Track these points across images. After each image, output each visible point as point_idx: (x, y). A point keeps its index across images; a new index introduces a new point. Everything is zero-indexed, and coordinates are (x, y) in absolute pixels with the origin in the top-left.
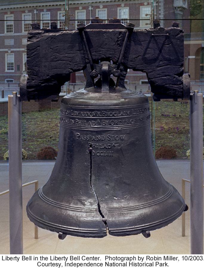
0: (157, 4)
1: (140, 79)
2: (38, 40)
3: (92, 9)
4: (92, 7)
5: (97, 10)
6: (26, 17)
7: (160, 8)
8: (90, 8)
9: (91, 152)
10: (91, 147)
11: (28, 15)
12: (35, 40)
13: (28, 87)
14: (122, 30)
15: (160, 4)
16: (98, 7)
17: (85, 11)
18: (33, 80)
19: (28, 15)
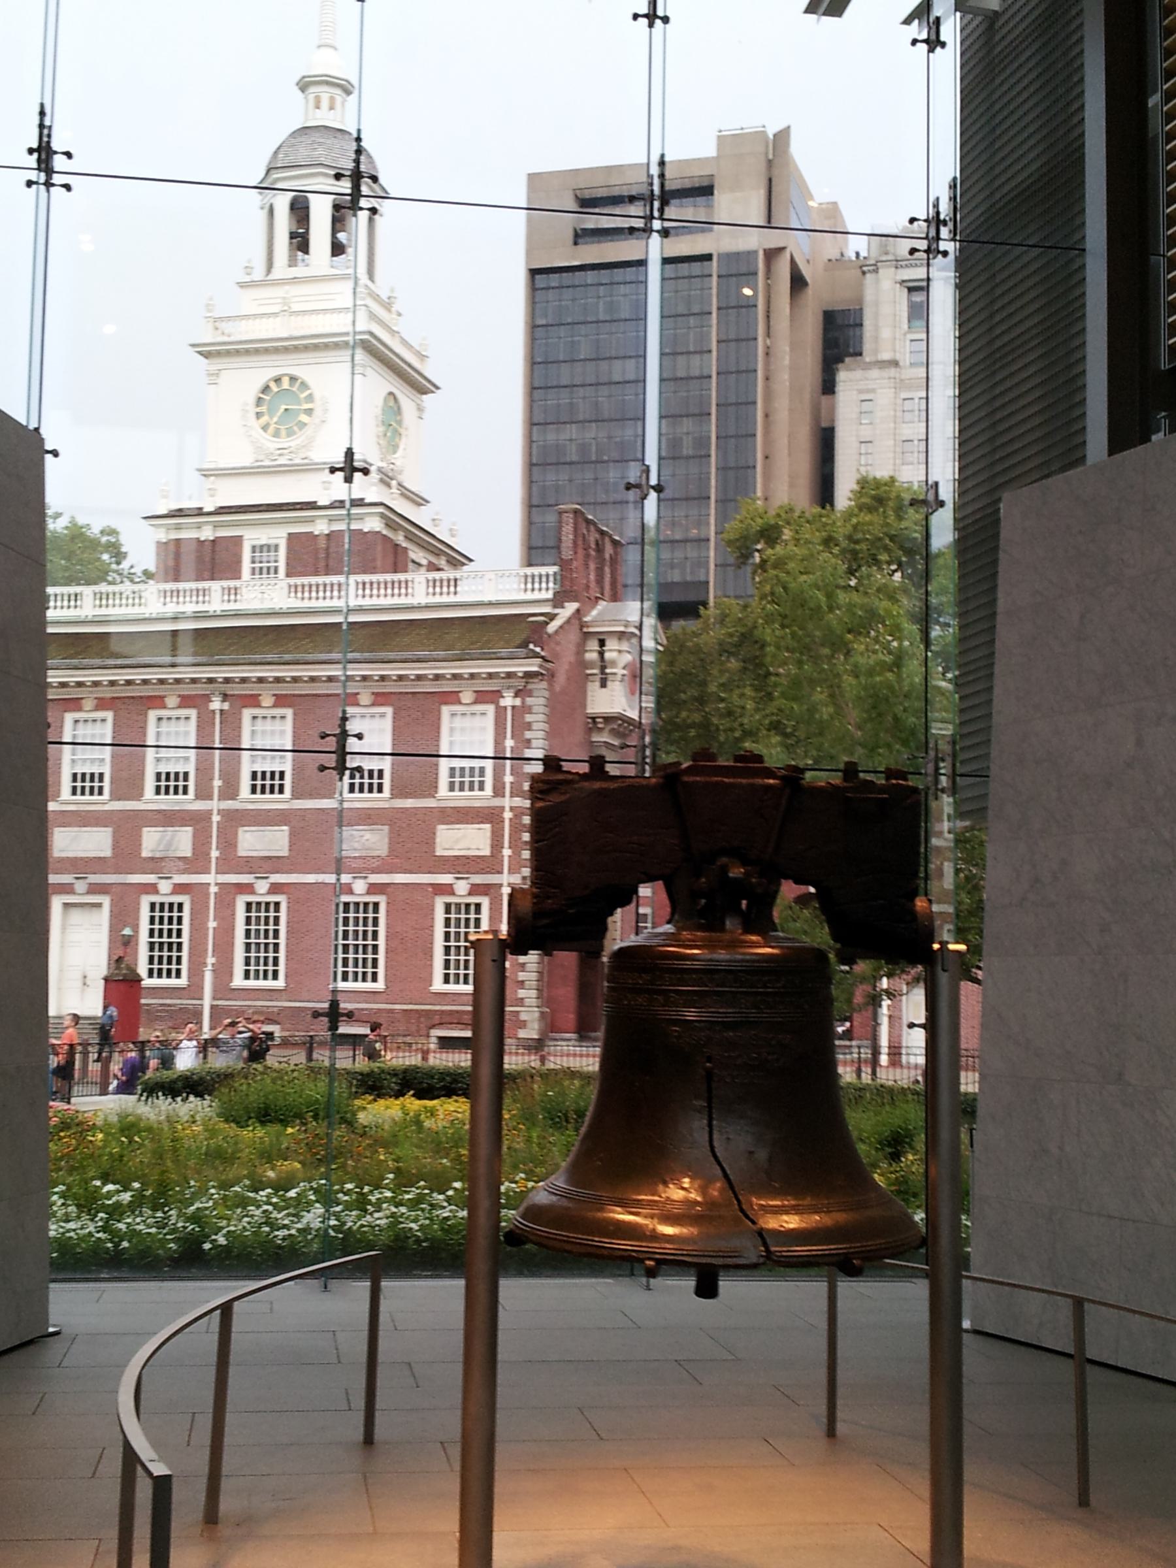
0: (518, 702)
1: (433, 1027)
2: (563, 798)
3: (226, 706)
4: (225, 697)
5: (247, 713)
6: (165, 727)
7: (529, 718)
8: (216, 704)
9: (709, 1075)
10: (709, 1059)
11: (86, 721)
12: (556, 798)
13: (538, 914)
14: (771, 781)
15: (529, 701)
16: (253, 701)
17: (193, 713)
18: (549, 898)
19: (95, 721)
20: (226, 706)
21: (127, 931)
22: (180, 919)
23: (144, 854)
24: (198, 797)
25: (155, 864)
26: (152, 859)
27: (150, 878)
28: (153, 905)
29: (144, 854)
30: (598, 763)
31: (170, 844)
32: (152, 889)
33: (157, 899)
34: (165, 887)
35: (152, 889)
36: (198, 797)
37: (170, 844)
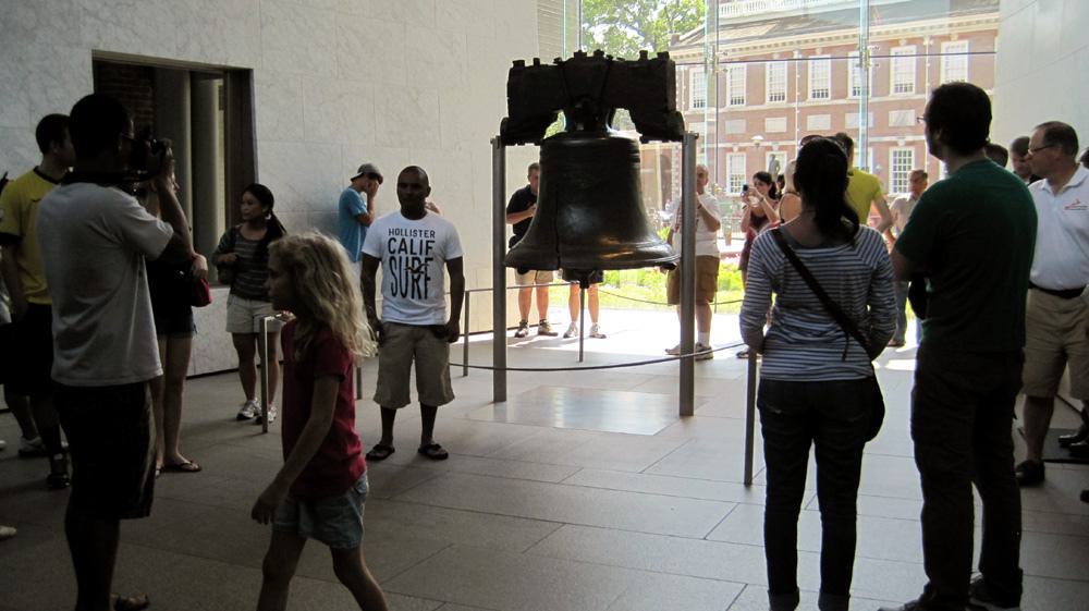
3: (932, 42)
4: (932, 38)
8: (926, 42)
20: (932, 42)
21: (878, 167)
22: (895, 162)
23: (891, 125)
24: (917, 92)
25: (898, 130)
26: (894, 128)
27: (894, 139)
28: (895, 154)
29: (891, 125)
30: (536, 61)
31: (903, 119)
32: (895, 144)
33: (898, 149)
34: (901, 142)
35: (895, 144)
36: (917, 92)
37: (903, 119)
